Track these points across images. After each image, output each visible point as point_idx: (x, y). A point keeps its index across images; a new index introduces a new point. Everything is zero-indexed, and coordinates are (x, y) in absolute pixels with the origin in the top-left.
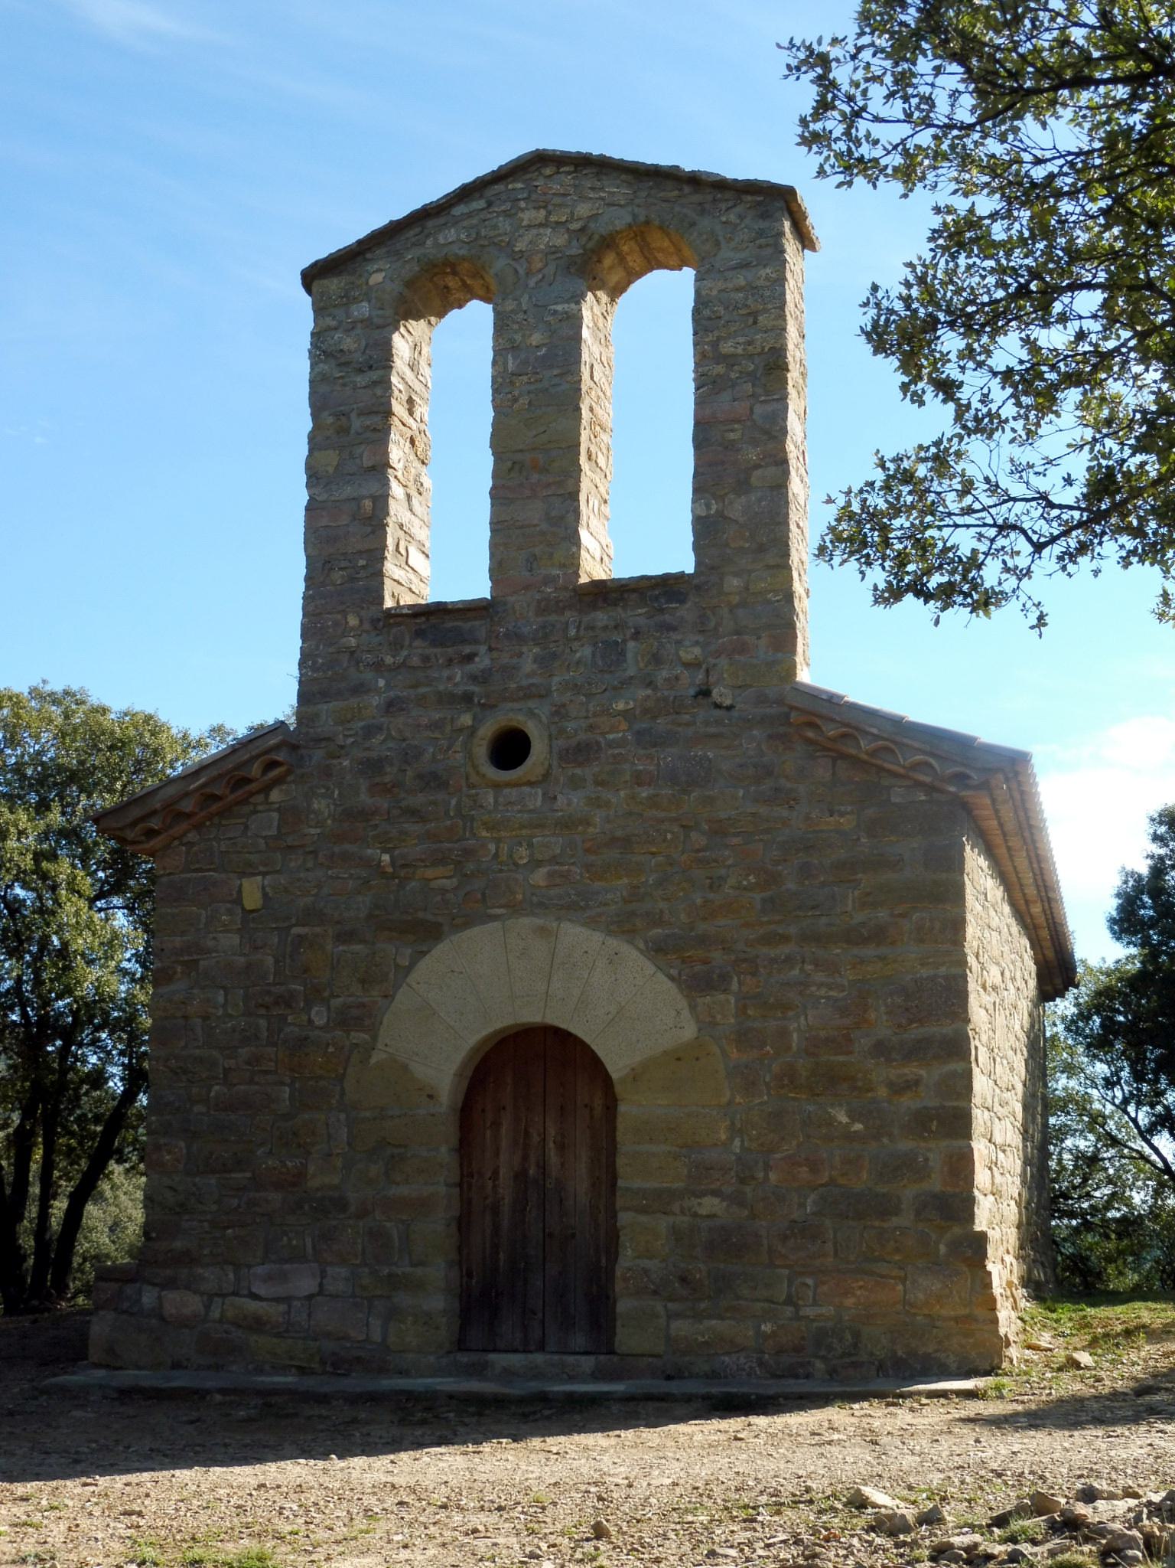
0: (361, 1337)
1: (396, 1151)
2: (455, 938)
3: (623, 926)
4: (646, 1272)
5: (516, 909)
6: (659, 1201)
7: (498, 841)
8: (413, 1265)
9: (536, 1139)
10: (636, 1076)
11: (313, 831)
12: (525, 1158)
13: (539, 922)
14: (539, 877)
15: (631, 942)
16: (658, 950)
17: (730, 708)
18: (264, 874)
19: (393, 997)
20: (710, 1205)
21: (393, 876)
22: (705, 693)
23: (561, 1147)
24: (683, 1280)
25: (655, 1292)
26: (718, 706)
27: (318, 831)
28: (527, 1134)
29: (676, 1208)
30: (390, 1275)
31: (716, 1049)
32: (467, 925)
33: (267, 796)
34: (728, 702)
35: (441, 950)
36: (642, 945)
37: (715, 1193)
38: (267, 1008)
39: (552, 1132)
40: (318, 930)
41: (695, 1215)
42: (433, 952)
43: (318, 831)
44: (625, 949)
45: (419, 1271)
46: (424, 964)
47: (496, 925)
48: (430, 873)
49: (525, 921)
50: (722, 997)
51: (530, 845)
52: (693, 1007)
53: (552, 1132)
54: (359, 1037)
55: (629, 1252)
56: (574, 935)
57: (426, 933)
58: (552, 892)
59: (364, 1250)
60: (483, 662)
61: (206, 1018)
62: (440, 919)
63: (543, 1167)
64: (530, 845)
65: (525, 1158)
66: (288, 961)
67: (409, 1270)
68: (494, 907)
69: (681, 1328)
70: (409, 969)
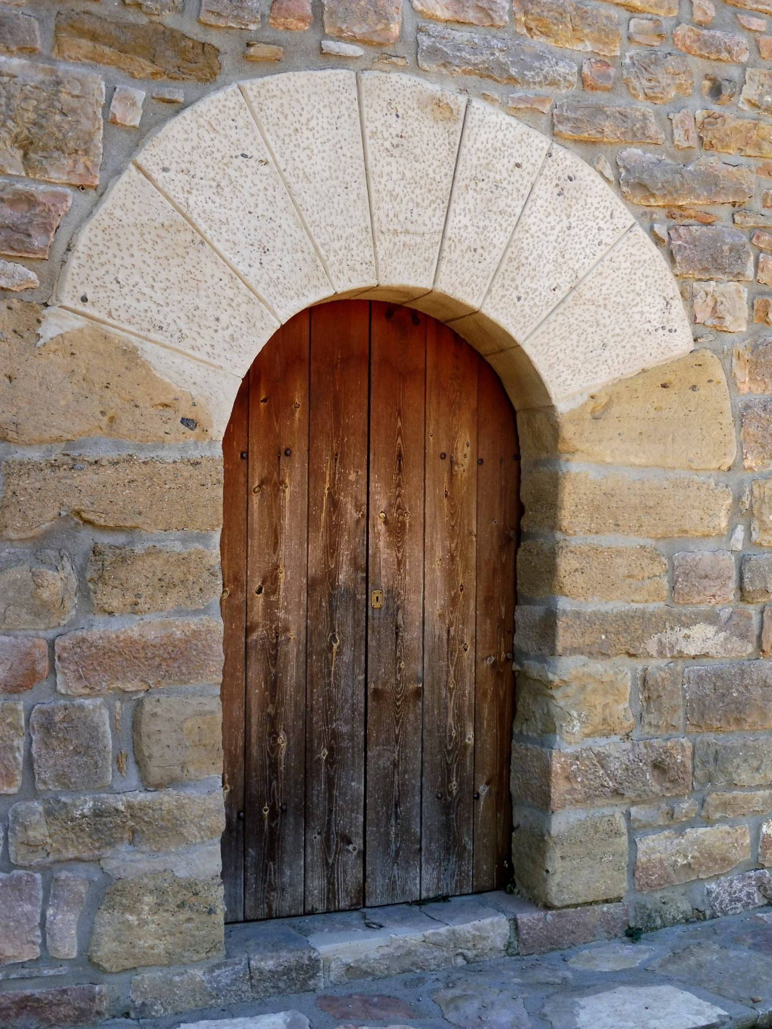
0: (31, 953)
1: (105, 540)
2: (252, 85)
3: (578, 127)
4: (602, 759)
5: (381, 52)
6: (623, 635)
8: (147, 785)
9: (351, 514)
10: (599, 409)
12: (331, 549)
13: (432, 87)
16: (634, 184)
19: (101, 192)
20: (702, 638)
23: (397, 531)
24: (658, 767)
25: (617, 793)
28: (335, 504)
29: (652, 646)
30: (98, 813)
31: (719, 374)
32: (276, 64)
35: (218, 104)
36: (609, 173)
37: (711, 618)
39: (380, 501)
41: (681, 655)
42: (202, 106)
44: (585, 172)
45: (167, 799)
46: (176, 129)
47: (343, 75)
50: (733, 285)
52: (688, 297)
53: (380, 501)
55: (577, 727)
58: (462, 35)
59: (29, 760)
62: (214, 39)
63: (364, 568)
65: (331, 549)
67: (142, 797)
68: (339, 38)
69: (656, 847)
70: (139, 136)
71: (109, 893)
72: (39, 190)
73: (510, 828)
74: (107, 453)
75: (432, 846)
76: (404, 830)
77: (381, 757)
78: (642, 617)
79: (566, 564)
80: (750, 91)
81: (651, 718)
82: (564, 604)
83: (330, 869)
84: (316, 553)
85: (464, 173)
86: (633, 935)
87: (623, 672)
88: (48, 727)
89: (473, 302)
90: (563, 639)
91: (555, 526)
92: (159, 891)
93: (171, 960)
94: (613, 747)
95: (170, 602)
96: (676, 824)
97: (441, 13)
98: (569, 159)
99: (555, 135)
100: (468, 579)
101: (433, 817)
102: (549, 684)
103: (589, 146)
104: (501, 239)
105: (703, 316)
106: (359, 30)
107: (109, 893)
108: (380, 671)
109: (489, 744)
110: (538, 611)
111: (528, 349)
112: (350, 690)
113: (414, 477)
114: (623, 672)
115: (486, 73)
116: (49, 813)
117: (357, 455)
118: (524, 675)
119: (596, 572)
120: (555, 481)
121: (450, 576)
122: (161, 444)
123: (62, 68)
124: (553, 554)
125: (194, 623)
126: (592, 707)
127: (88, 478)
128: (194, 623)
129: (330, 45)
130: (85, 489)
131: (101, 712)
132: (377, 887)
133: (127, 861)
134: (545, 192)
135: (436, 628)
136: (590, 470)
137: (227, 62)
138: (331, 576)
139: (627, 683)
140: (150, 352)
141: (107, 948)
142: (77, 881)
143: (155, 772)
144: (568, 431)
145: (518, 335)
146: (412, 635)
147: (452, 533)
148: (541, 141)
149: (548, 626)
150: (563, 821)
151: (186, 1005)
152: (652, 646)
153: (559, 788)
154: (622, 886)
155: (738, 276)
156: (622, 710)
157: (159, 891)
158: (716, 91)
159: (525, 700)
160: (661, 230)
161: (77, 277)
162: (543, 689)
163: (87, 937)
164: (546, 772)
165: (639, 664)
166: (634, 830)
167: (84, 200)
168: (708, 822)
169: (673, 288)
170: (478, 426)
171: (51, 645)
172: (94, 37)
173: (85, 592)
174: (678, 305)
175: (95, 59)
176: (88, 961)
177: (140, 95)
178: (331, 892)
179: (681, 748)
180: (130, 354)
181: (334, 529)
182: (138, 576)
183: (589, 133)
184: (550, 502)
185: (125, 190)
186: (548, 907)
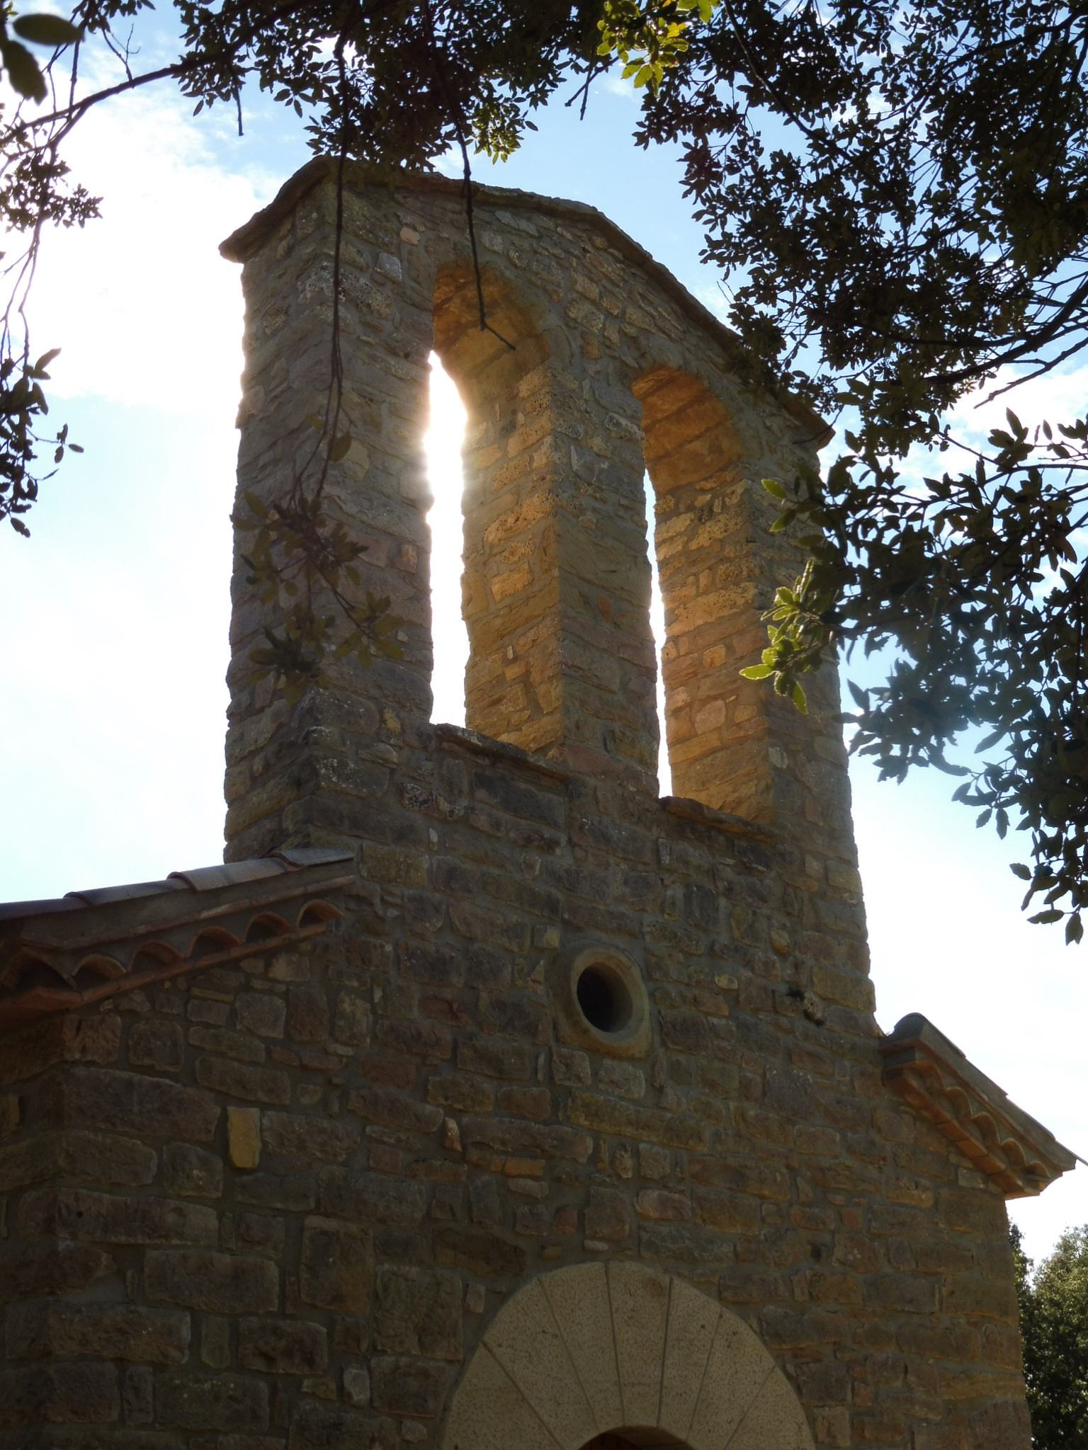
3: (733, 1293)
7: (597, 1136)
11: (341, 1050)
13: (649, 1271)
14: (650, 1201)
15: (745, 1318)
16: (771, 1334)
17: (819, 1023)
18: (264, 1107)
19: (463, 1364)
21: (463, 1158)
22: (796, 994)
26: (808, 1016)
27: (349, 1051)
32: (559, 1262)
33: (268, 965)
34: (819, 1015)
35: (528, 1292)
36: (755, 1326)
38: (270, 1360)
40: (354, 1228)
42: (519, 1296)
43: (349, 1051)
44: (743, 1328)
46: (507, 1313)
47: (597, 1266)
48: (513, 1165)
49: (630, 1266)
50: (839, 1410)
51: (636, 1154)
52: (812, 1421)
54: (416, 1430)
56: (687, 1296)
57: (504, 1263)
58: (664, 1229)
60: (563, 858)
61: (159, 1367)
64: (636, 1154)
66: (305, 1275)
68: (593, 1238)
70: (483, 1322)
80: (839, 1253)
97: (654, 1214)
98: (732, 1318)
99: (720, 1298)
103: (741, 1307)
105: (822, 1436)
129: (589, 1244)
148: (715, 1306)
155: (842, 1401)
158: (817, 1254)
160: (790, 1368)
169: (802, 1417)
174: (806, 1428)
177: (482, 1289)
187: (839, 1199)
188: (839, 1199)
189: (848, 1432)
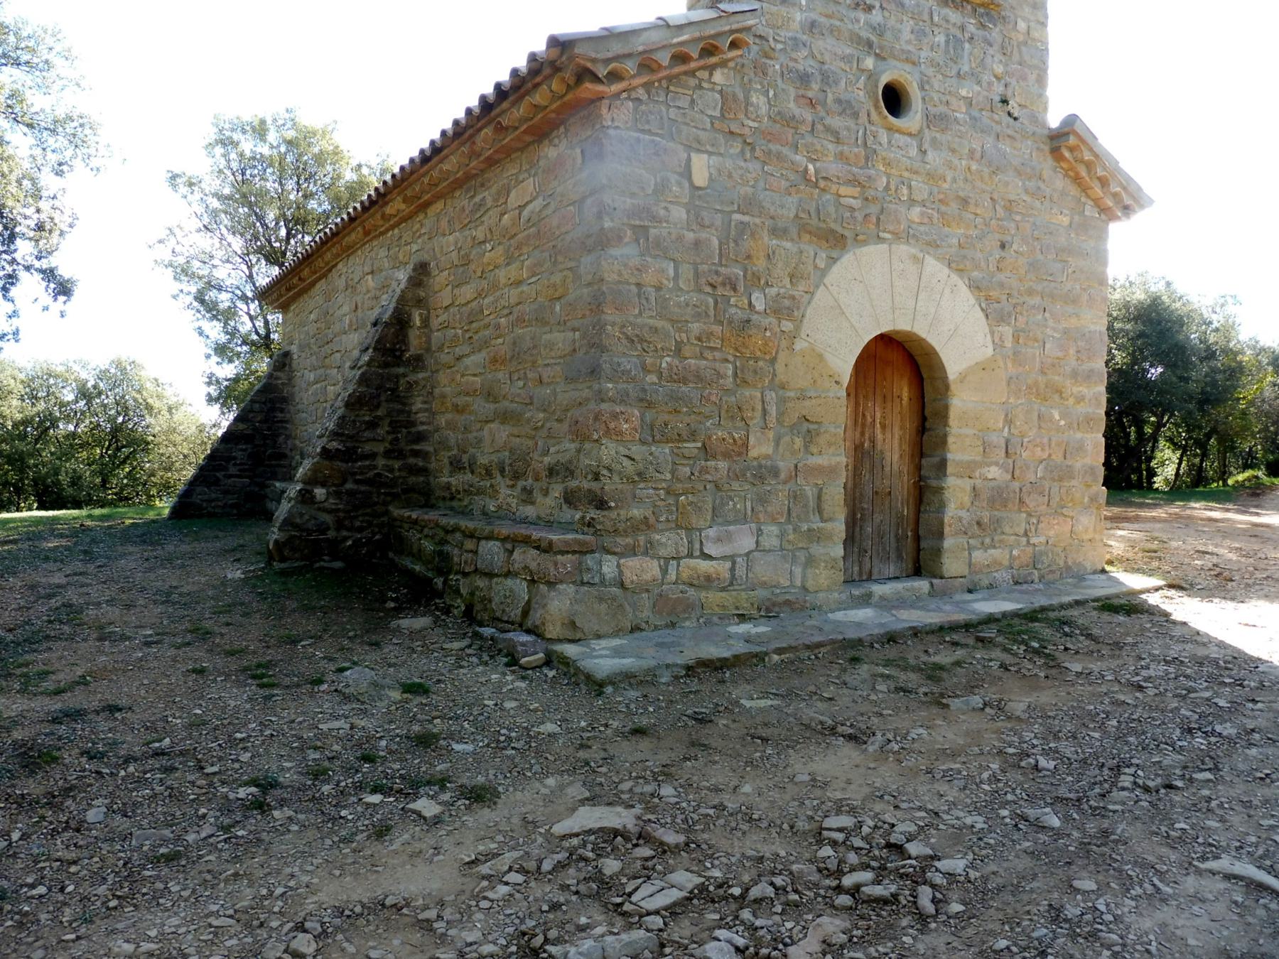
0: (788, 583)
1: (812, 427)
2: (858, 251)
3: (956, 265)
4: (960, 519)
5: (897, 236)
6: (969, 470)
7: (888, 176)
8: (823, 520)
9: (869, 419)
10: (963, 378)
11: (751, 124)
12: (863, 434)
13: (913, 251)
14: (915, 213)
15: (962, 278)
16: (975, 287)
17: (1015, 119)
18: (710, 154)
19: (813, 294)
20: (994, 472)
21: (816, 185)
22: (1005, 102)
23: (883, 427)
24: (978, 523)
25: (965, 533)
26: (1009, 114)
27: (756, 125)
28: (864, 415)
29: (977, 474)
30: (809, 530)
31: (1002, 365)
32: (865, 243)
33: (711, 75)
34: (1016, 115)
35: (847, 259)
37: (997, 464)
38: (714, 287)
39: (878, 415)
40: (757, 221)
41: (986, 479)
43: (756, 125)
44: (960, 283)
45: (828, 525)
46: (836, 269)
47: (885, 246)
48: (843, 190)
49: (903, 247)
51: (910, 187)
52: (992, 333)
53: (878, 415)
54: (787, 326)
55: (952, 505)
56: (933, 266)
57: (835, 242)
58: (922, 228)
59: (789, 510)
60: (876, 17)
61: (658, 288)
62: (846, 233)
63: (873, 441)
64: (910, 187)
65: (863, 434)
66: (732, 245)
67: (821, 525)
68: (884, 231)
69: (978, 556)
70: (824, 272)
71: (810, 561)
72: (796, 293)
73: (918, 550)
74: (812, 394)
75: (893, 556)
76: (884, 549)
77: (878, 518)
78: (974, 462)
79: (951, 440)
80: (1015, 247)
81: (976, 503)
82: (949, 456)
83: (860, 562)
84: (858, 435)
85: (922, 285)
86: (970, 591)
87: (967, 484)
88: (795, 497)
89: (923, 336)
90: (950, 470)
91: (946, 424)
92: (825, 561)
93: (829, 590)
94: (963, 514)
95: (831, 450)
96: (984, 547)
97: (917, 220)
98: (955, 278)
99: (949, 266)
100: (906, 447)
101: (894, 545)
102: (942, 488)
103: (960, 271)
104: (933, 310)
105: (996, 341)
106: (891, 228)
107: (810, 561)
108: (877, 483)
109: (912, 516)
110: (936, 460)
111: (941, 355)
112: (868, 492)
113: (889, 405)
114: (967, 484)
115: (929, 244)
116: (794, 530)
117: (871, 395)
118: (928, 487)
119: (961, 444)
120: (946, 407)
121: (900, 446)
122: (828, 391)
123: (802, 246)
124: (945, 436)
125: (838, 459)
126: (957, 497)
127: (807, 403)
128: (838, 459)
129: (881, 234)
130: (807, 407)
131: (810, 492)
132: (875, 571)
133: (817, 550)
134: (947, 291)
135: (895, 467)
136: (961, 402)
137: (849, 241)
138: (862, 444)
139: (968, 488)
140: (828, 356)
141: (810, 584)
142: (802, 556)
143: (825, 515)
144: (953, 387)
145: (938, 349)
146: (887, 469)
147: (901, 428)
148: (946, 271)
149: (942, 465)
150: (948, 543)
151: (833, 607)
152: (977, 474)
153: (947, 530)
154: (966, 572)
155: (1009, 324)
156: (967, 500)
157: (825, 561)
158: (1003, 246)
159: (928, 496)
160: (983, 305)
161: (806, 328)
162: (939, 490)
163: (804, 577)
164: (942, 523)
165: (972, 481)
166: (970, 549)
167: (807, 297)
168: (994, 547)
169: (987, 330)
170: (910, 385)
171: (796, 466)
172: (810, 233)
173: (806, 447)
174: (989, 336)
175: (810, 242)
176: (804, 588)
177: (824, 255)
178: (860, 573)
179: (986, 516)
180: (821, 357)
181: (863, 425)
182: (822, 440)
183: (961, 267)
184: (943, 415)
185: (821, 292)
186: (942, 578)
187: (1018, 218)
188: (1018, 218)
189: (1010, 338)
